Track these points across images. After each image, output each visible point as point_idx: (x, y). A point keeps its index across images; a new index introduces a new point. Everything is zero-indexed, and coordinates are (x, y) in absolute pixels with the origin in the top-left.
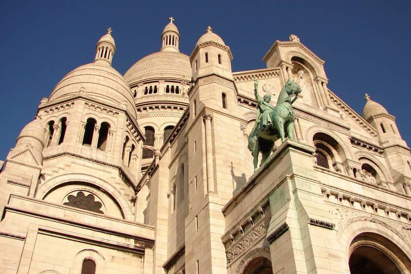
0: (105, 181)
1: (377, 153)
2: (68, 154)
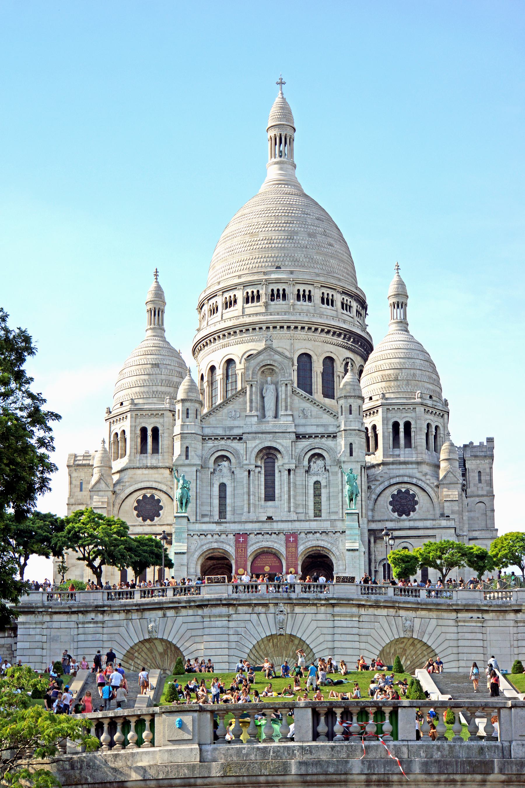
0: (159, 482)
1: (330, 439)
2: (129, 468)
